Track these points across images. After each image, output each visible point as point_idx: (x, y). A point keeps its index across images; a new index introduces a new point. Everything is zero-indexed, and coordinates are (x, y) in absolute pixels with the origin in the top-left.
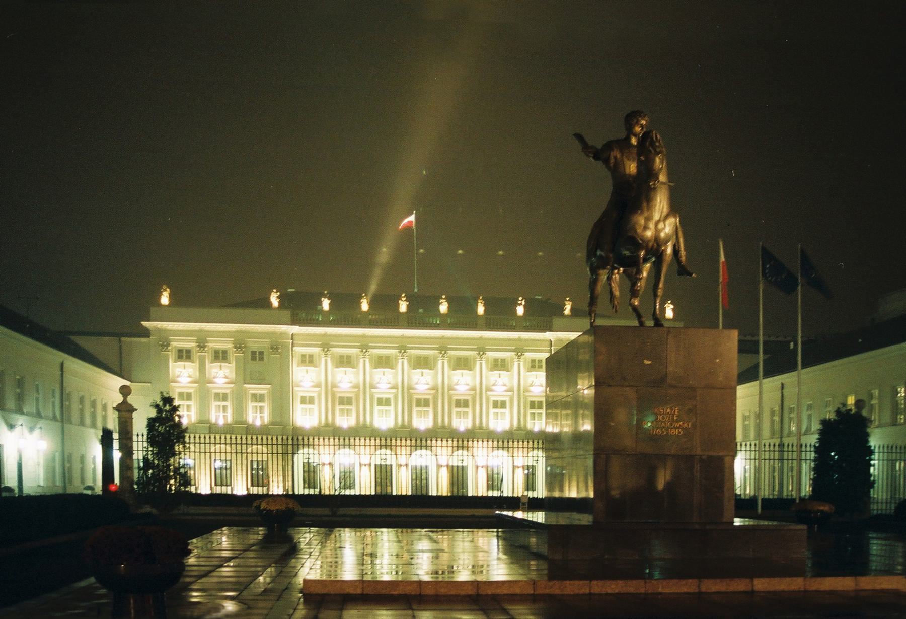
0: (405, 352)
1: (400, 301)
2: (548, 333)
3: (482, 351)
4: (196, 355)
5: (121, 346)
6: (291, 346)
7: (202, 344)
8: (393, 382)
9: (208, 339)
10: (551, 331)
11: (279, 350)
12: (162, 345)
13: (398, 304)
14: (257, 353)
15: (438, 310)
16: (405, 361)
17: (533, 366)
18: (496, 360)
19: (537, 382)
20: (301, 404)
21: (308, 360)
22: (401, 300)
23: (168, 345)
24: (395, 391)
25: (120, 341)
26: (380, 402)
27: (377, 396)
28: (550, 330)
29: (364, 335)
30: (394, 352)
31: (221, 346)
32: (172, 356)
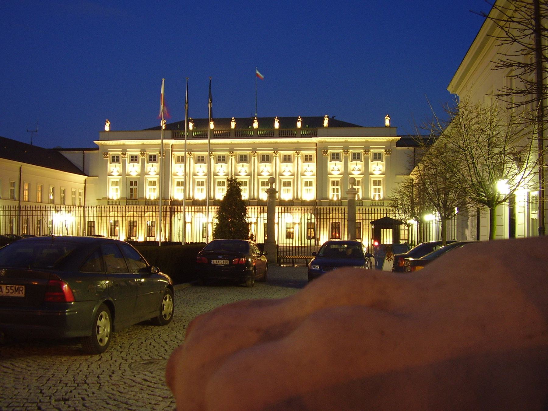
0: (233, 153)
1: (231, 122)
2: (313, 138)
3: (276, 150)
4: (121, 159)
5: (84, 156)
7: (124, 153)
8: (226, 171)
9: (127, 149)
11: (164, 155)
12: (105, 154)
14: (153, 156)
16: (233, 159)
17: (307, 159)
18: (285, 156)
19: (309, 169)
22: (232, 121)
23: (107, 154)
28: (316, 136)
30: (227, 153)
32: (109, 160)
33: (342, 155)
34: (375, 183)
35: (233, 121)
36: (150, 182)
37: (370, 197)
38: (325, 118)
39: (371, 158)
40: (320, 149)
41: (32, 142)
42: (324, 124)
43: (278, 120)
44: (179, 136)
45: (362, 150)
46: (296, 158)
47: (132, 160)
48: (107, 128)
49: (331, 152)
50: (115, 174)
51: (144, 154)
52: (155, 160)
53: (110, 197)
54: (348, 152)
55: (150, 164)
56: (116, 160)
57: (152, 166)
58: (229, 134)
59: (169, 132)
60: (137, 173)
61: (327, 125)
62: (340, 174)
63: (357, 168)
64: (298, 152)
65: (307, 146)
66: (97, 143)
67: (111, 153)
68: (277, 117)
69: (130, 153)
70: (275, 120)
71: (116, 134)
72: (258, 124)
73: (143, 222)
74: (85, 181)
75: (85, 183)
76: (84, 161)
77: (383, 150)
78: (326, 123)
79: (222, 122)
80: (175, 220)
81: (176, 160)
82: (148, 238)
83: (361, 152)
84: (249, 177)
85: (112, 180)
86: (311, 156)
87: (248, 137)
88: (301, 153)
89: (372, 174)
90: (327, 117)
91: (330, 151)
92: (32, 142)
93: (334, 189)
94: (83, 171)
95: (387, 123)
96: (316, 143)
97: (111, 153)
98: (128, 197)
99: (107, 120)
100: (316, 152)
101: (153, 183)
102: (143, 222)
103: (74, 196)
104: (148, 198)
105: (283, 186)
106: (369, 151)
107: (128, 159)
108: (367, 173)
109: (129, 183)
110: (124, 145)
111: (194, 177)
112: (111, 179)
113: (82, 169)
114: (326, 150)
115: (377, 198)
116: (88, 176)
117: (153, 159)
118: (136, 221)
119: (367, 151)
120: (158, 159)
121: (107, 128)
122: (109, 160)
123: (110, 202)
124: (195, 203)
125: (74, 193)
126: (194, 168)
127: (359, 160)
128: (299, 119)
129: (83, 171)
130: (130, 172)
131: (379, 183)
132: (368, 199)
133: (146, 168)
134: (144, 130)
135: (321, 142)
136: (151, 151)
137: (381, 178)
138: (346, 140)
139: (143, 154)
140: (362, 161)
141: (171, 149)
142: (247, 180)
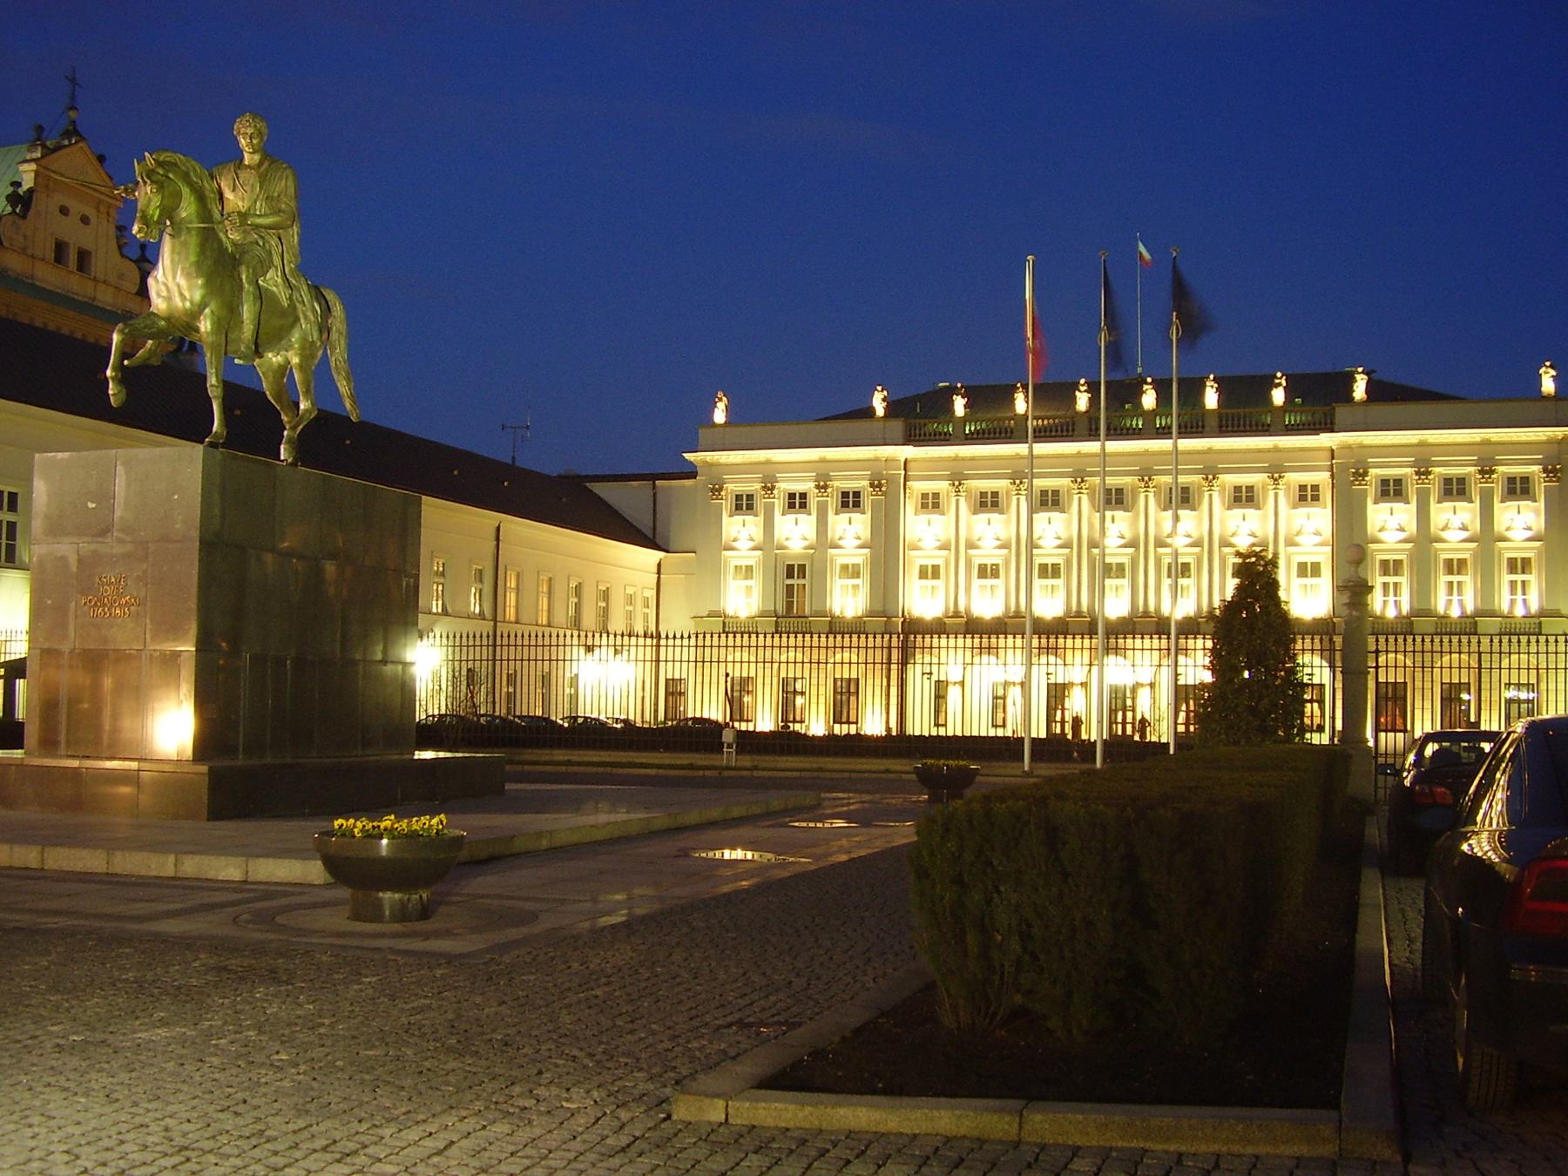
0: (1082, 481)
1: (1077, 393)
2: (1323, 435)
3: (1210, 473)
4: (759, 504)
5: (655, 494)
6: (902, 481)
7: (769, 485)
8: (1064, 535)
10: (1332, 431)
11: (883, 489)
12: (712, 490)
13: (1075, 398)
15: (1140, 405)
16: (1085, 498)
17: (1302, 498)
18: (1237, 489)
20: (920, 578)
21: (931, 503)
22: (1080, 391)
23: (721, 489)
24: (1066, 551)
25: (654, 486)
26: (983, 572)
27: (977, 562)
28: (1331, 429)
29: (1017, 455)
30: (1066, 482)
31: (798, 487)
32: (727, 505)
33: (1412, 485)
34: (1513, 566)
35: (1083, 388)
36: (845, 568)
37: (1496, 607)
38: (1358, 377)
39: (1498, 490)
40: (1344, 467)
41: (514, 458)
42: (1355, 394)
43: (1216, 385)
44: (925, 435)
45: (1472, 469)
46: (1271, 493)
47: (791, 506)
48: (720, 416)
49: (1377, 476)
50: (744, 545)
51: (825, 487)
52: (857, 504)
53: (730, 612)
54: (1430, 473)
55: (844, 517)
56: (747, 504)
57: (850, 523)
58: (1070, 428)
59: (897, 426)
60: (806, 543)
61: (1365, 396)
62: (1405, 541)
63: (1456, 522)
64: (1276, 475)
65: (1302, 460)
66: (692, 459)
67: (732, 488)
68: (1212, 377)
69: (785, 486)
70: (1208, 383)
71: (744, 432)
72: (1155, 395)
73: (822, 681)
74: (659, 565)
75: (659, 572)
76: (655, 511)
77: (1536, 468)
78: (1360, 390)
79: (1054, 393)
80: (914, 673)
81: (917, 501)
82: (837, 727)
83: (1469, 474)
84: (1131, 550)
85: (733, 563)
86: (1315, 488)
87: (1127, 434)
88: (1284, 480)
89: (1505, 539)
90: (1363, 372)
91: (1373, 471)
92: (514, 458)
93: (1451, 583)
94: (651, 537)
95: (1548, 385)
96: (1332, 451)
97: (732, 488)
98: (781, 610)
99: (720, 395)
100: (1332, 476)
101: (851, 571)
102: (822, 681)
103: (631, 608)
104: (837, 613)
105: (1298, 576)
106: (1492, 472)
107: (779, 503)
108: (1487, 537)
109: (782, 572)
110: (768, 462)
111: (971, 552)
112: (733, 559)
113: (649, 534)
114: (1361, 471)
115: (1519, 611)
116: (667, 551)
117: (850, 501)
118: (1405, 683)
119: (1486, 471)
120: (867, 501)
121: (720, 416)
122: (727, 505)
123: (730, 629)
124: (973, 627)
125: (630, 600)
126: (969, 527)
127: (1526, 496)
128: (1277, 381)
129: (651, 537)
130: (787, 539)
131: (1524, 565)
132: (1493, 614)
133: (833, 529)
134: (826, 419)
135: (1348, 448)
136: (846, 478)
137: (1531, 551)
138: (1423, 438)
139: (822, 488)
140: (1471, 501)
141: (903, 472)
142: (1126, 560)
